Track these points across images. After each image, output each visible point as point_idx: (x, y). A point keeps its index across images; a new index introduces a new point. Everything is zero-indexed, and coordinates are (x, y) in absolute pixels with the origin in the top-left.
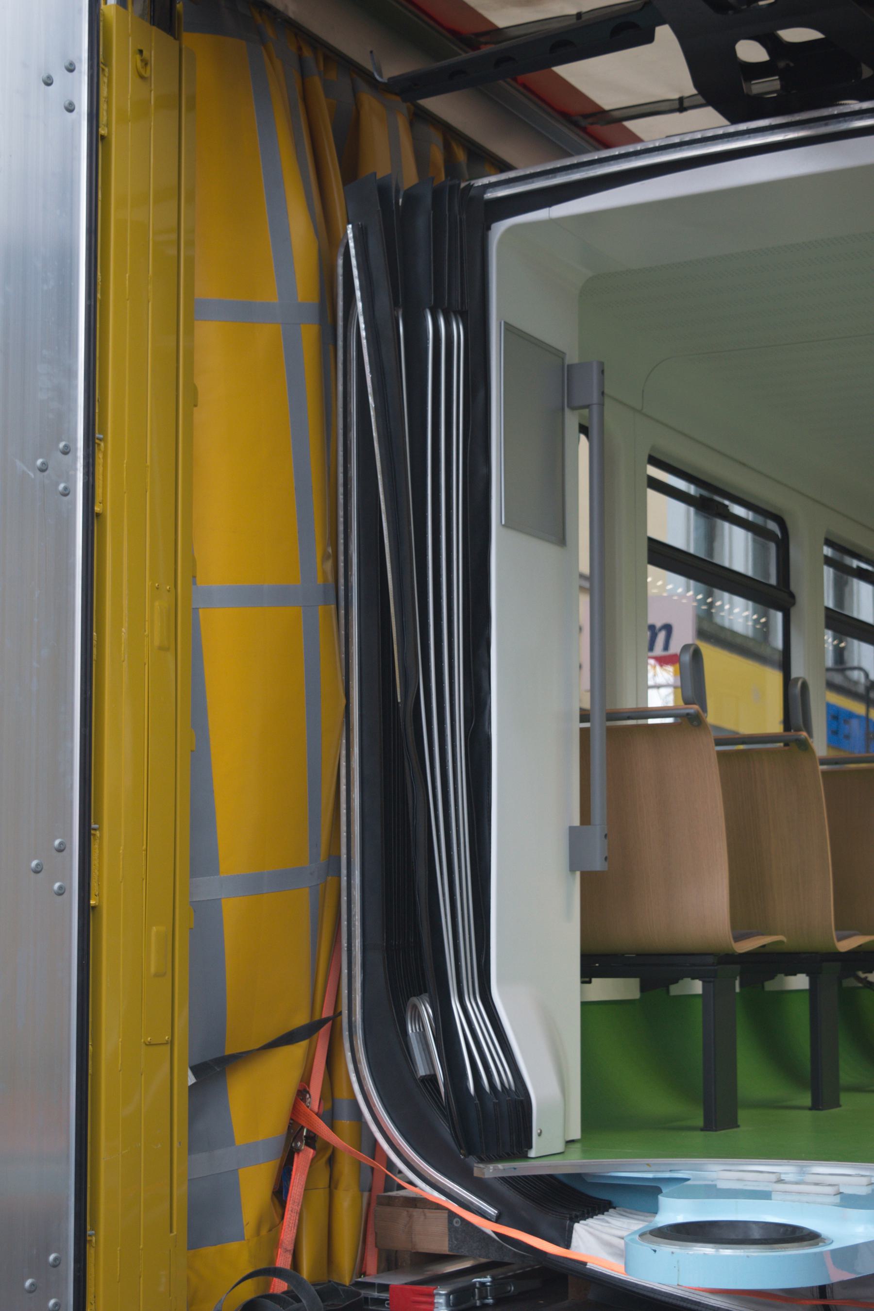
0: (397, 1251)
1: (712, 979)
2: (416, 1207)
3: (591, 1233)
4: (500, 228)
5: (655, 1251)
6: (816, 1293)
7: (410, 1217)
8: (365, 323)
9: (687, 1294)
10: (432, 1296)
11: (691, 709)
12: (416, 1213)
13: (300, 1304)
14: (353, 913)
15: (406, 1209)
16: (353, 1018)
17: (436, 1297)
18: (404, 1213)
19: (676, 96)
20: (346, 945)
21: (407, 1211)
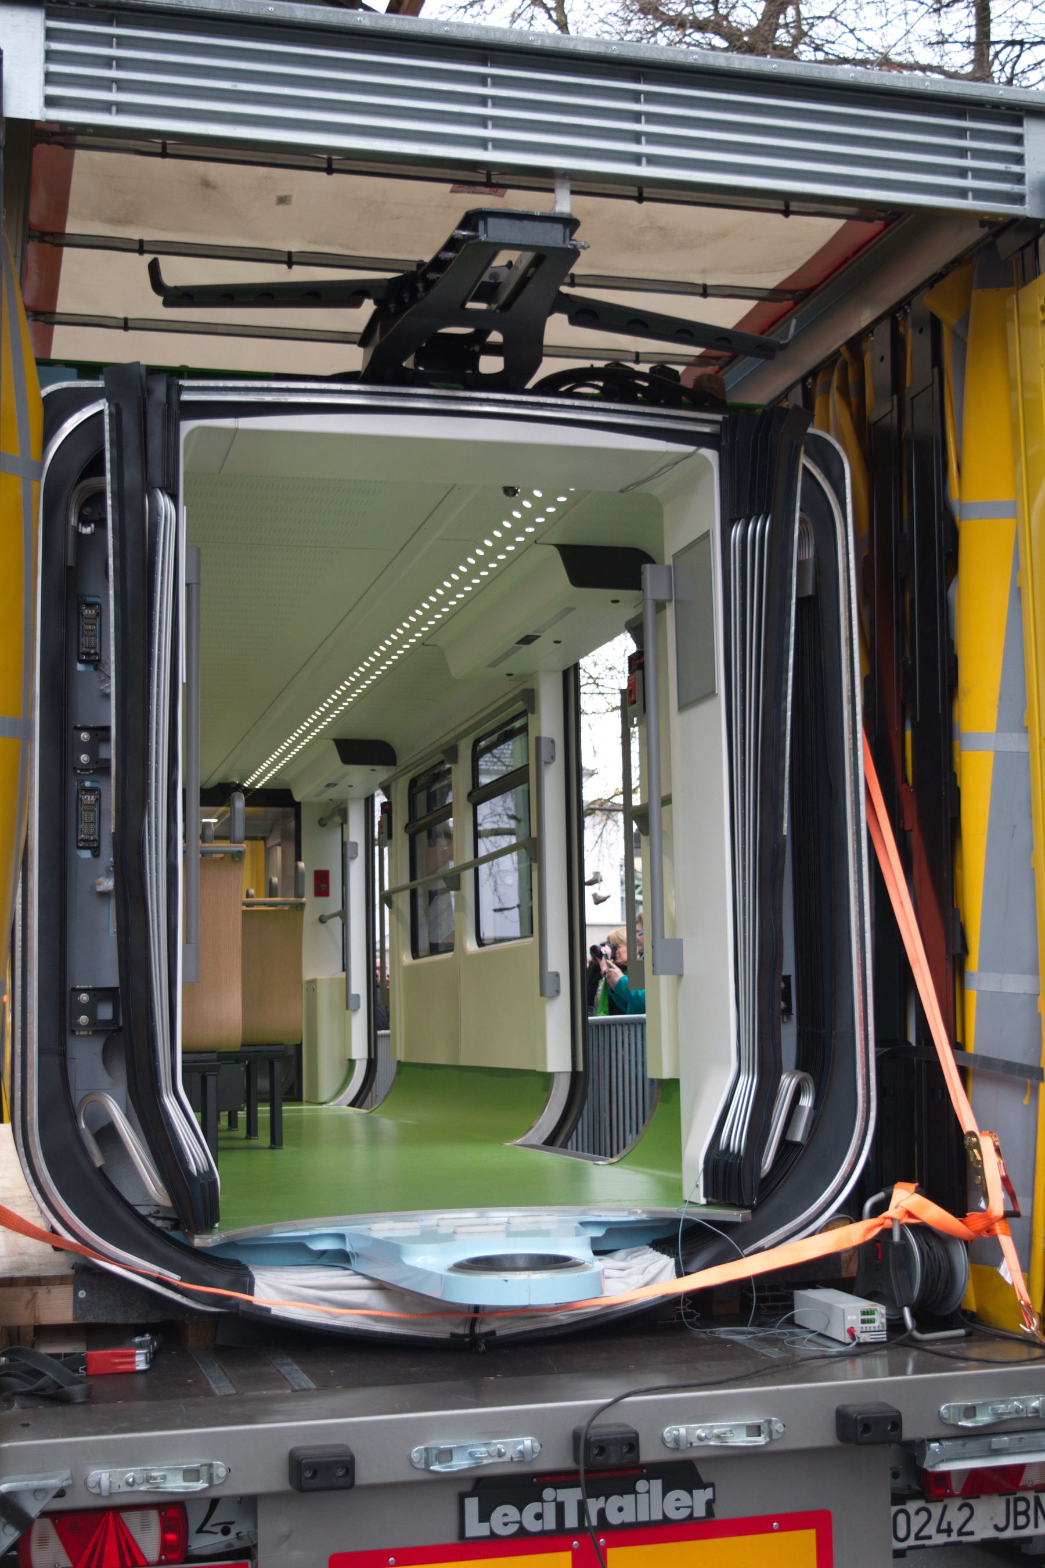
0: (19, 1327)
1: (216, 1073)
2: (40, 1285)
3: (270, 1286)
4: (187, 426)
5: (506, 1281)
6: (472, 1310)
7: (35, 1295)
8: (112, 492)
9: (356, 1324)
10: (133, 1355)
11: (242, 847)
12: (41, 1291)
13: (42, 1381)
14: (29, 1021)
15: (31, 1287)
16: (28, 1118)
17: (137, 1356)
18: (25, 1293)
19: (121, 316)
20: (20, 1051)
21: (32, 1290)
